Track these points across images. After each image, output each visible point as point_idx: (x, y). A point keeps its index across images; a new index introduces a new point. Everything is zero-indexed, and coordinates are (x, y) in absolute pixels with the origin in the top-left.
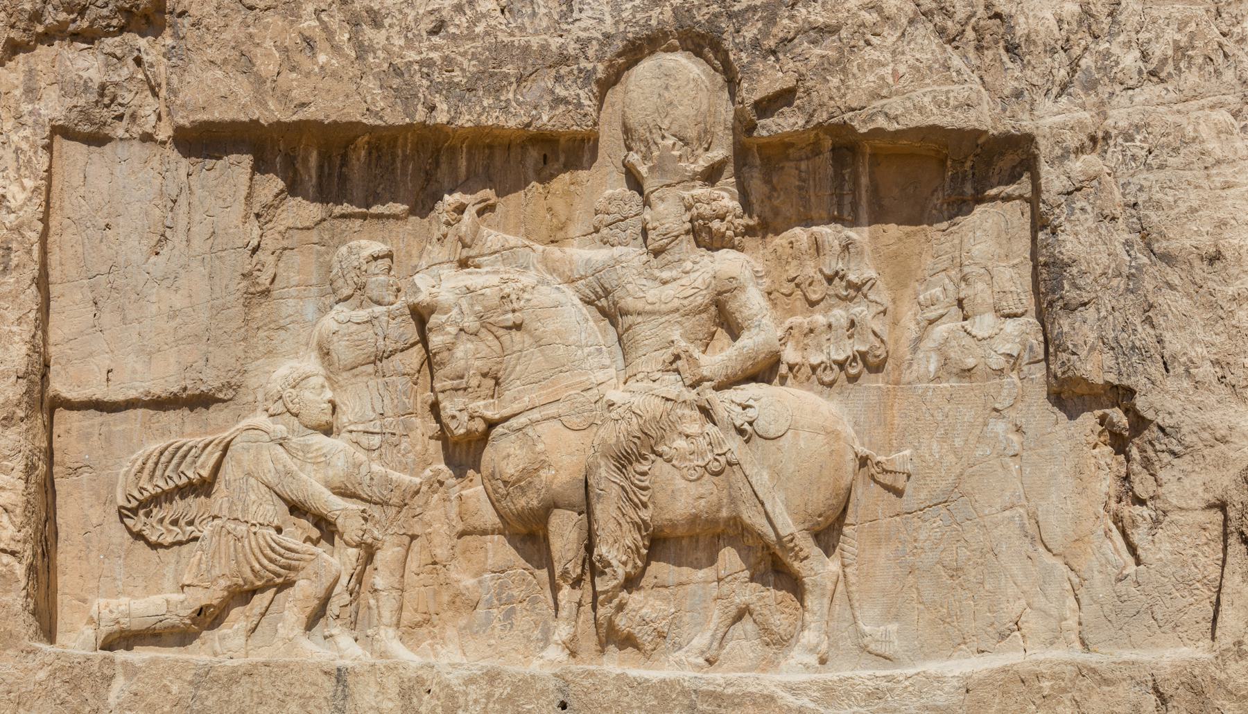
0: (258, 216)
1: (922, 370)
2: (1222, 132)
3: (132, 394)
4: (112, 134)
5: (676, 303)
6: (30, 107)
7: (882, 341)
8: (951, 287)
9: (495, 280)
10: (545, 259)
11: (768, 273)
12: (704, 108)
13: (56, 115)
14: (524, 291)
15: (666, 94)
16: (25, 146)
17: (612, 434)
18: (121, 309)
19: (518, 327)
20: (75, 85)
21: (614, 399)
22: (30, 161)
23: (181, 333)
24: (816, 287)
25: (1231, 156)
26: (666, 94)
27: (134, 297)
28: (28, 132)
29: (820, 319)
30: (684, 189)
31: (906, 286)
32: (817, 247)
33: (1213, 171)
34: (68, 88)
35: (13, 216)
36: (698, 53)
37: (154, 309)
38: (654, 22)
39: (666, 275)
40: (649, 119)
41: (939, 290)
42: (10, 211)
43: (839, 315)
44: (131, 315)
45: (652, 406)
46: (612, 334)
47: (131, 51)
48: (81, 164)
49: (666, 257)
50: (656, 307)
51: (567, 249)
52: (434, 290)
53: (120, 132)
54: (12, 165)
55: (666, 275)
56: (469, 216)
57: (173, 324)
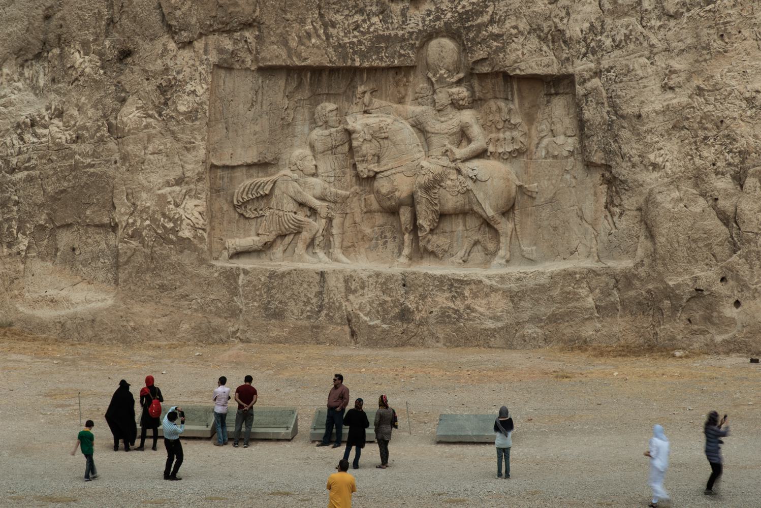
0: (287, 96)
1: (540, 155)
2: (644, 66)
3: (240, 163)
4: (234, 67)
5: (446, 131)
6: (206, 57)
7: (524, 145)
8: (548, 125)
9: (377, 120)
10: (396, 111)
11: (482, 118)
12: (456, 59)
13: (215, 60)
14: (388, 125)
15: (442, 54)
16: (203, 72)
17: (422, 180)
18: (236, 131)
19: (386, 138)
20: (222, 49)
21: (424, 165)
22: (205, 77)
23: (259, 140)
24: (500, 124)
25: (646, 75)
26: (442, 54)
27: (241, 126)
28: (204, 67)
29: (501, 135)
30: (449, 88)
31: (533, 124)
32: (499, 110)
33: (640, 82)
34: (221, 51)
35: (198, 98)
36: (454, 39)
37: (248, 131)
38: (437, 27)
39: (443, 119)
40: (436, 63)
41: (545, 126)
42: (197, 96)
43: (508, 135)
44: (240, 133)
45: (437, 169)
46: (423, 139)
47: (243, 38)
48: (223, 77)
49: (444, 113)
50: (439, 131)
51: (405, 106)
52: (354, 124)
53: (238, 67)
54: (198, 78)
55: (443, 119)
56: (367, 96)
57: (256, 137)
